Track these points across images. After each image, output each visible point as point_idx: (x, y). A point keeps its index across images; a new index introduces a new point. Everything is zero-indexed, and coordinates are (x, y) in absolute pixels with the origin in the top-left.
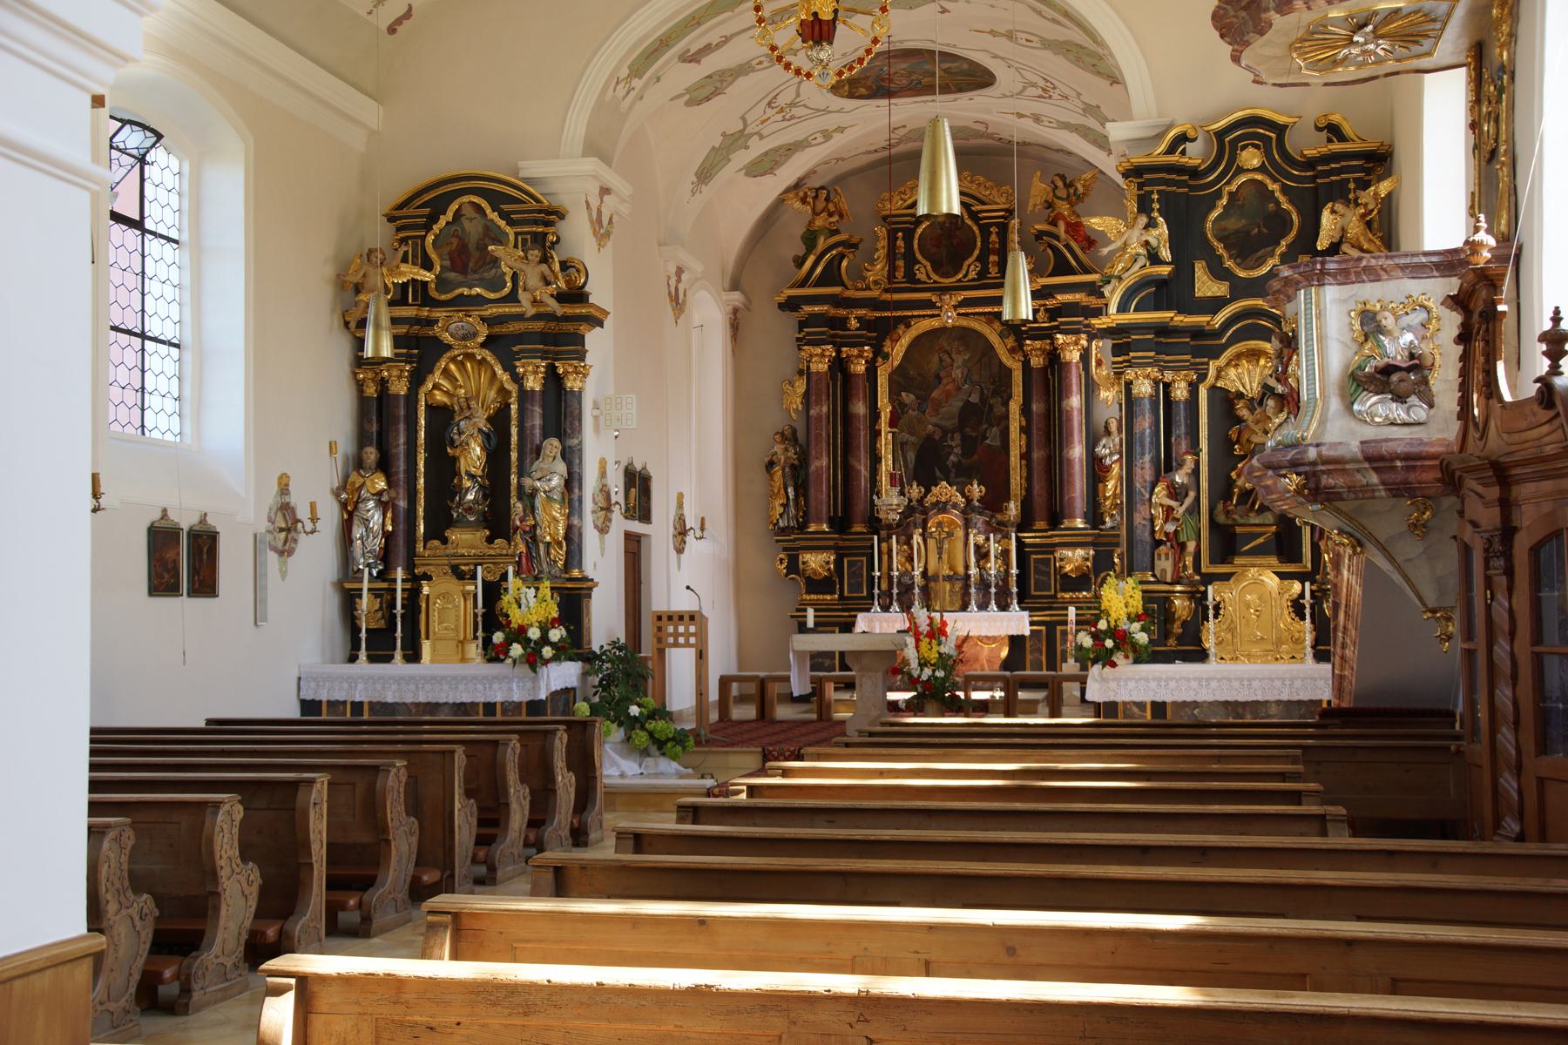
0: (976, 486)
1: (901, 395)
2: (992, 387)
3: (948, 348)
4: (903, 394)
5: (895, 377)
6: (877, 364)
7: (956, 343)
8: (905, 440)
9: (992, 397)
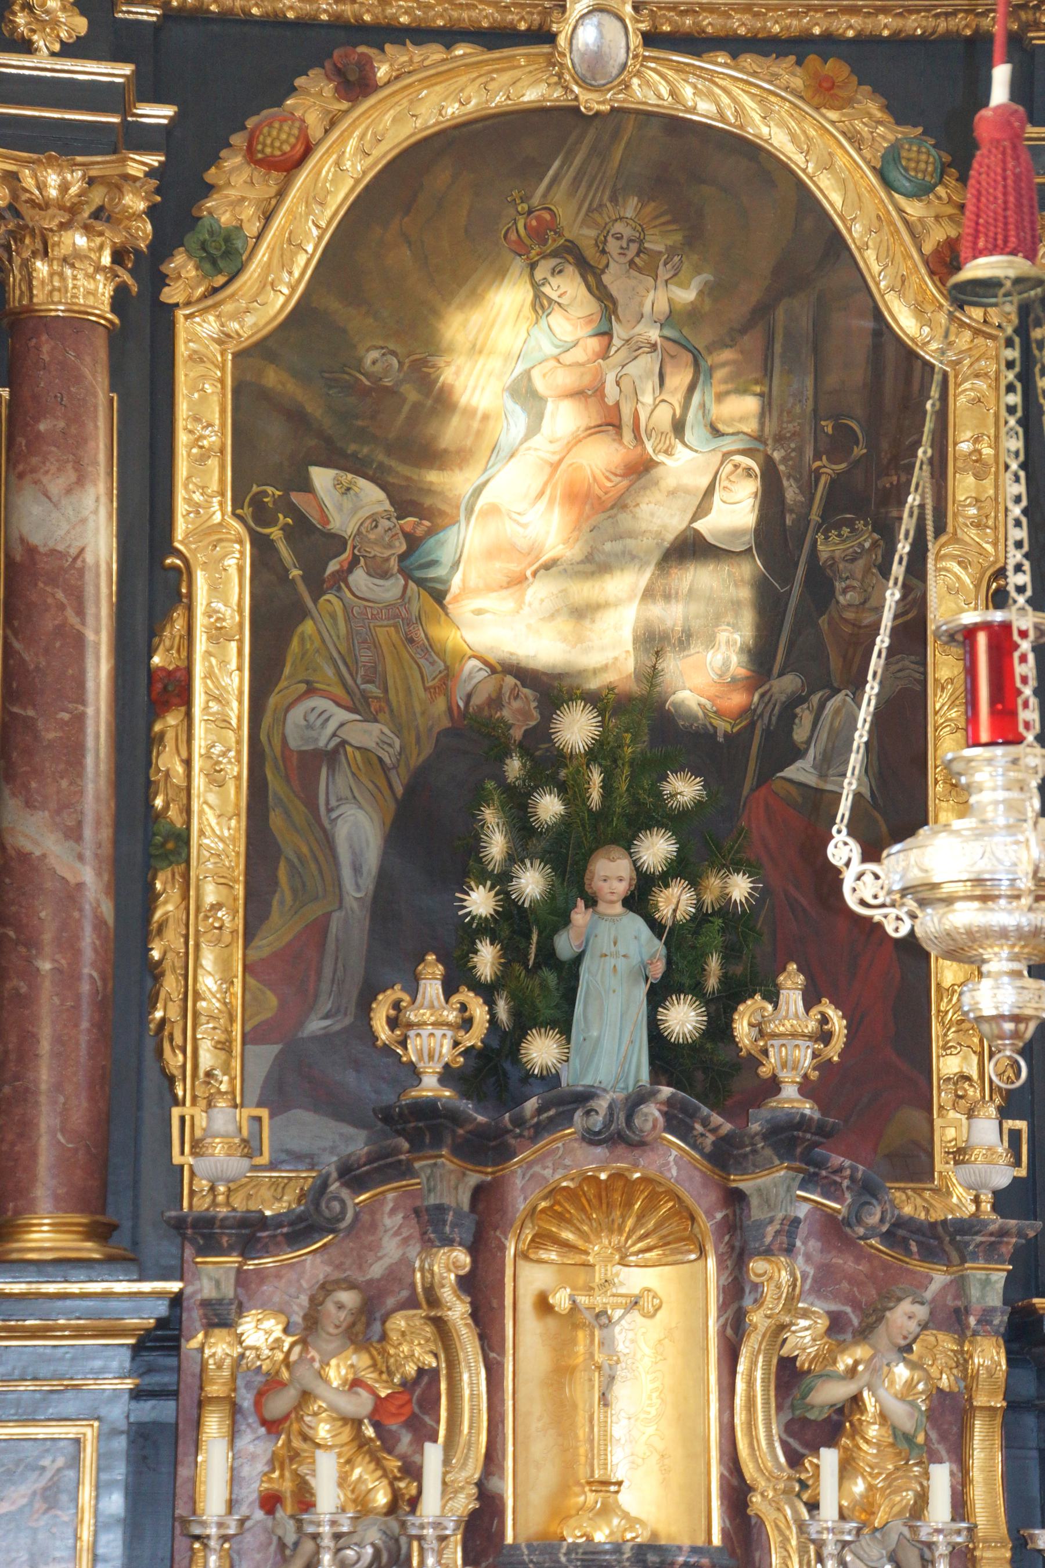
0: (792, 997)
1: (306, 486)
2: (829, 469)
3: (585, 236)
4: (322, 477)
5: (272, 378)
6: (171, 294)
7: (630, 207)
8: (323, 740)
9: (829, 522)
